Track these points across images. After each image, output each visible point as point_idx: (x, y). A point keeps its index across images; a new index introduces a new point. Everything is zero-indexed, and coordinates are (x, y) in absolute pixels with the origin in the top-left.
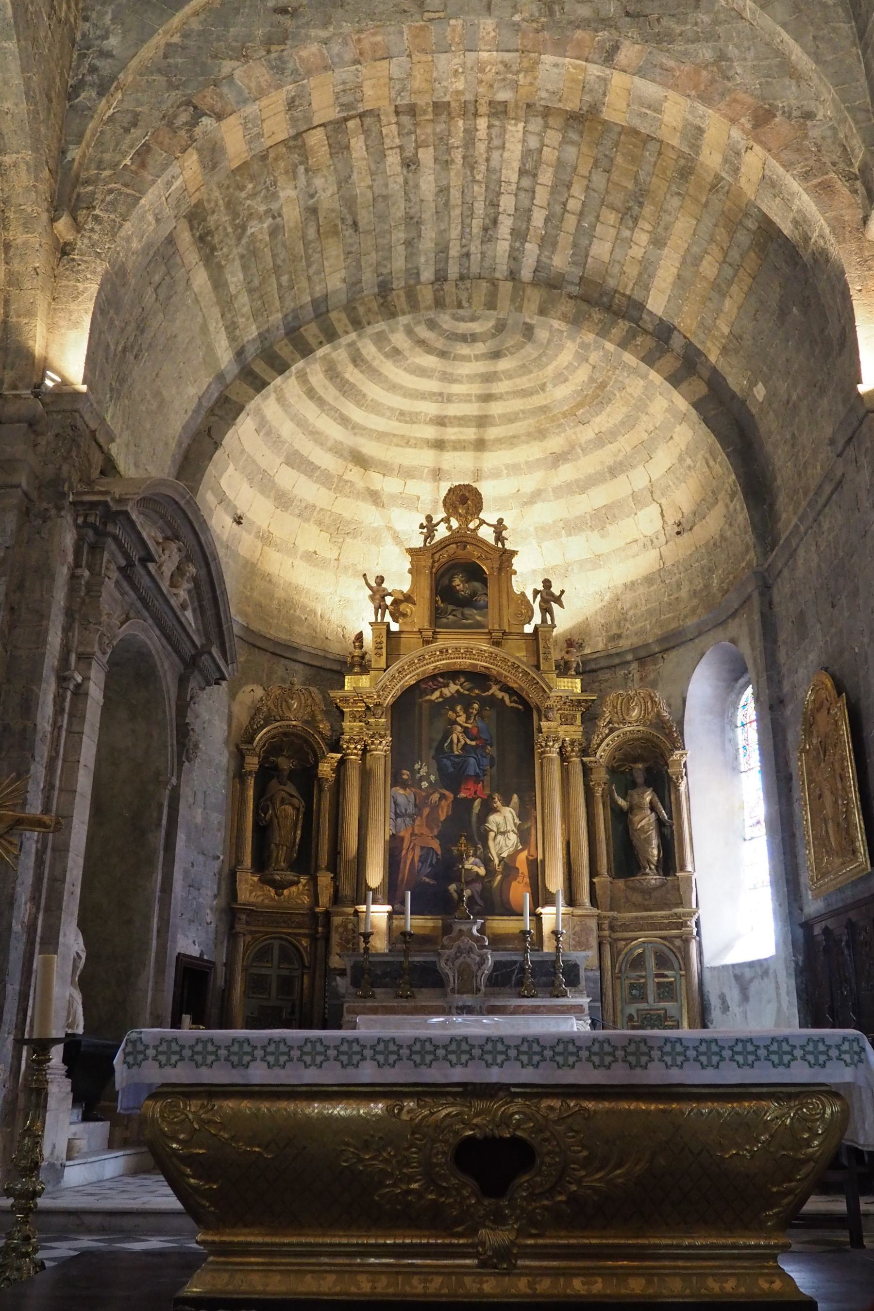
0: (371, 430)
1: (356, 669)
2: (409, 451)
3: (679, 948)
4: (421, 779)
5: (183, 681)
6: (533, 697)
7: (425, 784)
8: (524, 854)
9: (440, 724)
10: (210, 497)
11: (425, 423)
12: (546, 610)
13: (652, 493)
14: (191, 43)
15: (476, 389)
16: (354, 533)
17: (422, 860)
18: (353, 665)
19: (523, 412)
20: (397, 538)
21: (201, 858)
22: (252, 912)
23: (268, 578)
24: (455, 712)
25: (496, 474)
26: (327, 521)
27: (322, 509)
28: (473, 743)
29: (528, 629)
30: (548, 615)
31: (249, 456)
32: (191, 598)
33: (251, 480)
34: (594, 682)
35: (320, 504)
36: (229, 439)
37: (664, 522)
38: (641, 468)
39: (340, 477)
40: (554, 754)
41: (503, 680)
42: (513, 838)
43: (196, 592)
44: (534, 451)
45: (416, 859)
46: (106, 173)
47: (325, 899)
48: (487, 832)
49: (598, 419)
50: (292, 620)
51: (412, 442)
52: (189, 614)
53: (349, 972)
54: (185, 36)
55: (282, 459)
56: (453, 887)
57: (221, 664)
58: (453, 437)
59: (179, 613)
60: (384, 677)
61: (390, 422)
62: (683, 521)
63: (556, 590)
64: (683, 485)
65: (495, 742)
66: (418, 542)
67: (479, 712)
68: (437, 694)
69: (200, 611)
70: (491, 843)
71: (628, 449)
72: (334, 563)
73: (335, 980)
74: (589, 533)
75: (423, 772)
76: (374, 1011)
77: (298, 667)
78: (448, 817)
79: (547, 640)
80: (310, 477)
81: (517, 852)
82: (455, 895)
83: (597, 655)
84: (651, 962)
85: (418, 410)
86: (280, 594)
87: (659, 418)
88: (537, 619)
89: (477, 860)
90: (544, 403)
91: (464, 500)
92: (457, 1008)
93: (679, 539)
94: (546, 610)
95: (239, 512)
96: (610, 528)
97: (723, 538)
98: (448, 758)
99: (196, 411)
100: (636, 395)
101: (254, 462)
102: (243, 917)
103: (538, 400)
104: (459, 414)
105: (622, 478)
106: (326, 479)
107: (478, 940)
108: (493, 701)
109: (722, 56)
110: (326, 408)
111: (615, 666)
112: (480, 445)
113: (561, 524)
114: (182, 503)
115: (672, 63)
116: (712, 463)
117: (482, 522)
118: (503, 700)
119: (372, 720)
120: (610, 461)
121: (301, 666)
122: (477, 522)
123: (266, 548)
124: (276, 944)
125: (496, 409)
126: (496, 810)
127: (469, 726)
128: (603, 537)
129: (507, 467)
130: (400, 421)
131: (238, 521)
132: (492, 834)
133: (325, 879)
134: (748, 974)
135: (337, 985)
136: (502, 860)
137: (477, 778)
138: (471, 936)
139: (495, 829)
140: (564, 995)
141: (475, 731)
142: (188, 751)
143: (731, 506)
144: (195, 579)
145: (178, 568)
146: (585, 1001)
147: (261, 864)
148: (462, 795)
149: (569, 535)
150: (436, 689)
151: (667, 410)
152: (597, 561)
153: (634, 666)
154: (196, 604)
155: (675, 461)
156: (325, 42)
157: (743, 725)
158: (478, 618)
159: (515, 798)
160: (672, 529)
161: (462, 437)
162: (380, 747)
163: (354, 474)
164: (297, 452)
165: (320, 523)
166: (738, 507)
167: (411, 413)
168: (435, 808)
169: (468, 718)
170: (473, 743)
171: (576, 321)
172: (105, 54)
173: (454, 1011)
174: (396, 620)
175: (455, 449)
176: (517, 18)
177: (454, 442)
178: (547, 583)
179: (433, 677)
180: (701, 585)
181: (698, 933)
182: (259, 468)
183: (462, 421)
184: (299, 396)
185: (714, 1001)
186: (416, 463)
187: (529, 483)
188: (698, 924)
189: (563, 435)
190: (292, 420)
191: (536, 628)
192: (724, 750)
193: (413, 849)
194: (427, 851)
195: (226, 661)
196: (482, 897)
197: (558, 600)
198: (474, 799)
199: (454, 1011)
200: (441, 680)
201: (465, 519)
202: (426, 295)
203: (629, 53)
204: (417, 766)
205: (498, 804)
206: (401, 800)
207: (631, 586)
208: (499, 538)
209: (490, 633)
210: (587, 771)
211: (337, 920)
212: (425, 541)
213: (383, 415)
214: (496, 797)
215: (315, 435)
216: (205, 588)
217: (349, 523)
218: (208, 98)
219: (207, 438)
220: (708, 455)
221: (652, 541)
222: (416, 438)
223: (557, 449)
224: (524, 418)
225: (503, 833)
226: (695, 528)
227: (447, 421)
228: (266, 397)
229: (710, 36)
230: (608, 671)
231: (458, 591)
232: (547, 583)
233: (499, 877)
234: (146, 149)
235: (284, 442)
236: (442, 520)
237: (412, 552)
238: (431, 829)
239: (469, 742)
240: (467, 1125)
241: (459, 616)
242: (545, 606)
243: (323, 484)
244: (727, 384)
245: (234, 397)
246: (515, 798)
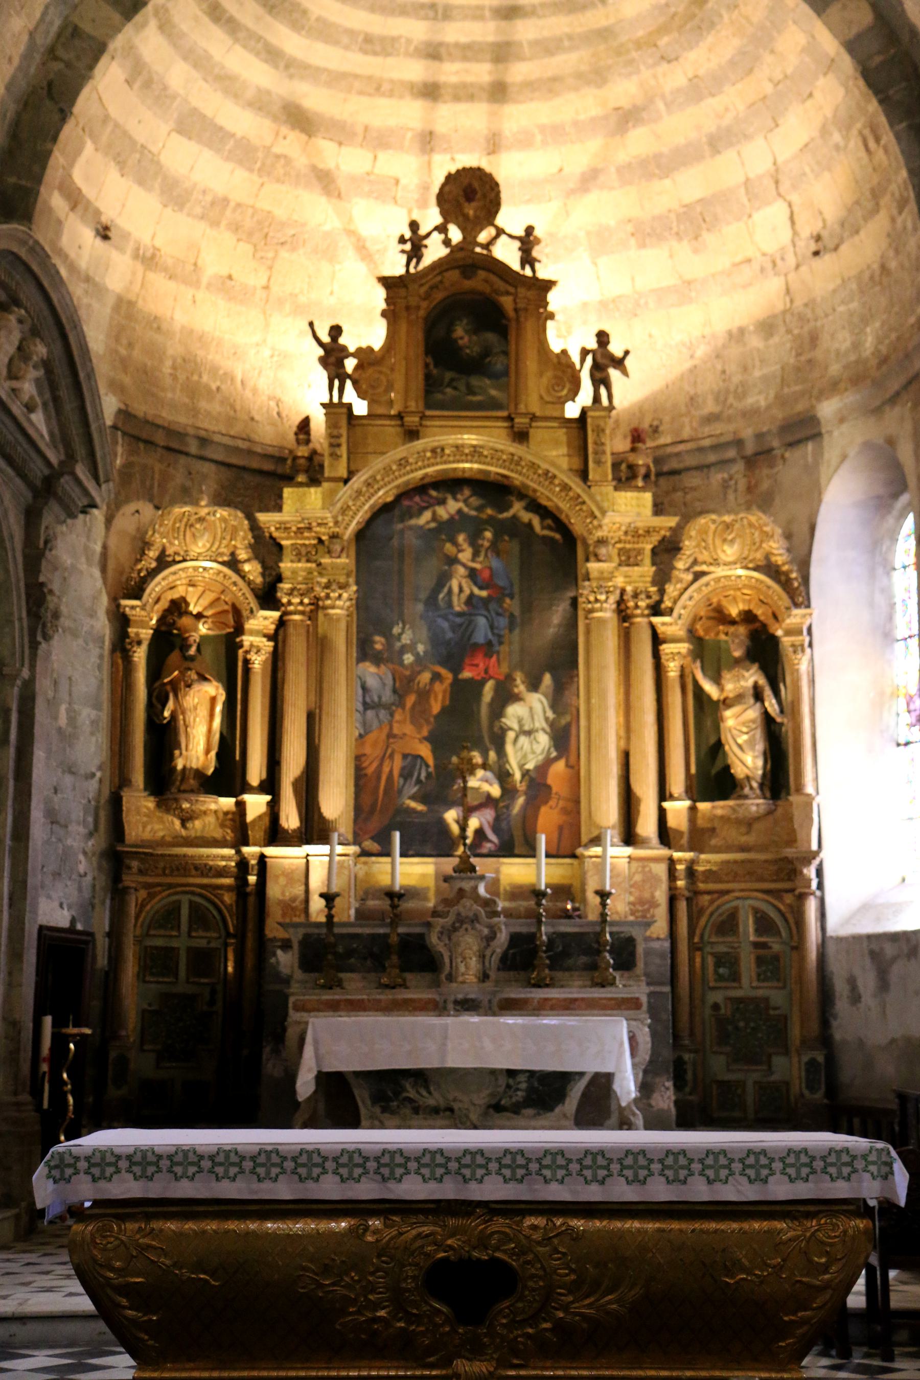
0: (318, 69)
1: (301, 478)
2: (383, 102)
3: (790, 906)
4: (403, 650)
5: (32, 516)
6: (577, 525)
7: (408, 658)
8: (560, 766)
9: (433, 565)
10: (57, 202)
11: (407, 54)
12: (600, 379)
13: (777, 182)
16: (292, 243)
17: (406, 774)
18: (296, 470)
19: (570, 37)
20: (363, 250)
21: (68, 780)
23: (155, 324)
24: (455, 544)
25: (525, 142)
26: (248, 223)
27: (239, 205)
28: (484, 593)
29: (572, 410)
30: (603, 391)
31: (117, 125)
32: (40, 394)
33: (122, 165)
34: (675, 490)
35: (236, 197)
36: (85, 104)
37: (795, 233)
38: (760, 141)
39: (268, 149)
40: (607, 612)
41: (531, 493)
42: (544, 740)
43: (50, 382)
45: (396, 773)
48: (504, 731)
49: (692, 55)
50: (193, 390)
51: (386, 87)
52: (38, 418)
53: (296, 946)
55: (172, 124)
56: (451, 816)
57: (90, 485)
58: (454, 79)
59: (22, 419)
60: (345, 493)
61: (349, 55)
62: (825, 234)
63: (616, 348)
64: (827, 175)
65: (516, 589)
66: (396, 266)
67: (494, 544)
68: (427, 515)
69: (55, 404)
70: (509, 749)
71: (741, 107)
72: (260, 294)
73: (274, 954)
74: (674, 243)
75: (406, 639)
76: (334, 1007)
77: (207, 468)
78: (444, 710)
79: (600, 431)
80: (218, 151)
81: (547, 763)
82: (455, 829)
83: (681, 447)
84: (748, 926)
85: (394, 33)
86: (174, 349)
87: (792, 62)
88: (585, 396)
89: (489, 774)
90: (604, 23)
91: (469, 194)
92: (456, 1002)
93: (817, 263)
94: (600, 379)
95: (104, 219)
96: (708, 238)
97: (884, 268)
98: (445, 617)
99: (27, 56)
100: (755, 20)
101: (125, 133)
102: (135, 864)
104: (463, 39)
105: (730, 155)
107: (488, 904)
108: (514, 528)
110: (241, 35)
111: (708, 466)
113: (630, 228)
114: (23, 253)
116: (872, 144)
117: (500, 232)
118: (530, 525)
119: (326, 560)
120: (710, 126)
121: (213, 467)
122: (492, 231)
123: (151, 276)
124: (185, 899)
126: (517, 698)
127: (477, 566)
128: (696, 251)
129: (543, 129)
130: (365, 52)
131: (104, 233)
132: (511, 735)
134: (889, 950)
135: (278, 962)
136: (525, 774)
137: (488, 649)
138: (476, 897)
139: (516, 726)
140: (612, 983)
141: (486, 574)
142: (44, 626)
143: (899, 220)
144: (46, 364)
145: (20, 348)
146: (641, 991)
148: (466, 674)
149: (642, 245)
150: (426, 508)
151: (803, 50)
153: (738, 468)
154: (48, 396)
155: (815, 134)
157: (904, 567)
158: (493, 392)
159: (547, 679)
160: (807, 246)
161: (470, 79)
162: (338, 603)
164: (195, 111)
165: (236, 228)
166: (909, 225)
167: (383, 39)
168: (424, 695)
169: (476, 554)
170: (484, 593)
173: (450, 1006)
174: (361, 395)
175: (457, 98)
177: (455, 87)
178: (603, 338)
179: (421, 488)
180: (848, 344)
181: (820, 886)
182: (133, 142)
183: (468, 52)
184: (196, 19)
185: (840, 987)
186: (392, 122)
188: (819, 873)
189: (635, 78)
190: (185, 58)
191: (584, 412)
192: (871, 604)
193: (391, 756)
195: (96, 478)
196: (496, 829)
197: (619, 363)
198: (482, 683)
199: (450, 1006)
200: (434, 493)
201: (470, 228)
204: (396, 630)
205: (520, 687)
206: (372, 682)
207: (738, 336)
208: (528, 259)
209: (510, 419)
210: (657, 640)
212: (408, 265)
213: (336, 43)
214: (519, 677)
216: (61, 370)
217: (283, 225)
219: (48, 102)
220: (867, 132)
221: (774, 263)
222: (392, 81)
223: (625, 103)
224: (571, 49)
225: (529, 733)
226: (843, 248)
227: (443, 51)
228: (144, 25)
230: (694, 473)
231: (461, 348)
232: (603, 338)
233: (521, 801)
235: (174, 97)
236: (437, 228)
237: (387, 282)
238: (419, 728)
239: (476, 591)
240: (439, 1245)
241: (463, 388)
242: (598, 375)
243: (240, 162)
244: (903, 11)
245: (86, 27)
246: (547, 679)
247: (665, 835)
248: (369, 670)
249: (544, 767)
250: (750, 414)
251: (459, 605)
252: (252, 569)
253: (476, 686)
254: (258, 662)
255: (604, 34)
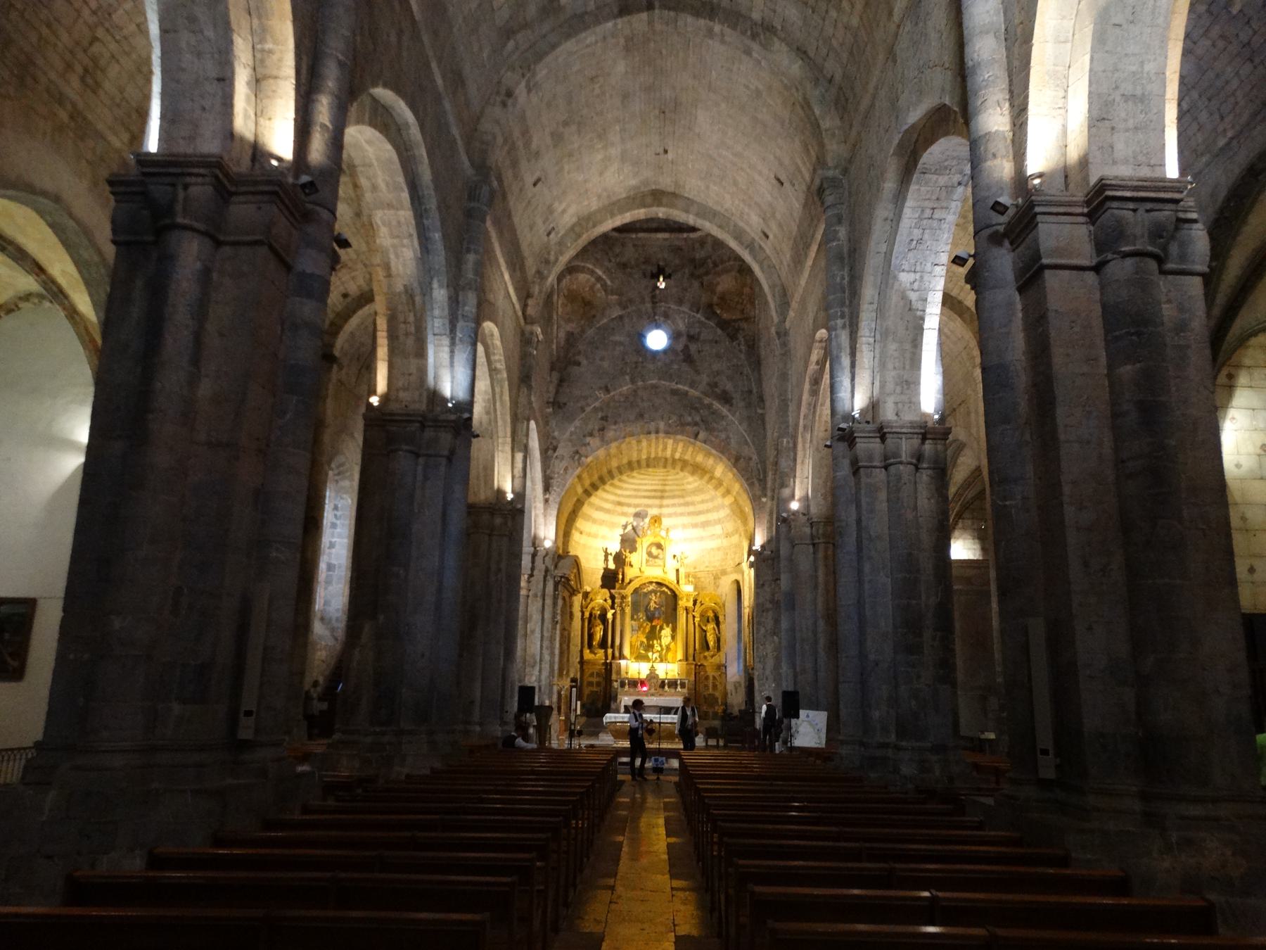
6: (677, 592)
14: (578, 431)
15: (661, 482)
17: (641, 645)
22: (589, 662)
42: (669, 638)
44: (681, 501)
46: (556, 476)
47: (610, 657)
54: (576, 428)
103: (682, 487)
106: (608, 511)
108: (664, 592)
109: (728, 437)
112: (662, 497)
115: (713, 439)
120: (705, 508)
125: (667, 488)
133: (610, 651)
134: (737, 685)
137: (659, 618)
147: (590, 646)
152: (702, 538)
156: (615, 430)
163: (619, 509)
168: (645, 628)
171: (693, 473)
172: (554, 438)
176: (670, 422)
187: (679, 510)
194: (642, 643)
202: (644, 463)
203: (702, 435)
210: (694, 617)
211: (614, 666)
215: (607, 501)
218: (583, 450)
229: (726, 429)
234: (566, 469)
247: (694, 660)
248: (633, 622)
249: (669, 644)
250: (715, 567)
251: (652, 609)
252: (610, 601)
253: (655, 627)
254: (610, 621)
255: (684, 490)
